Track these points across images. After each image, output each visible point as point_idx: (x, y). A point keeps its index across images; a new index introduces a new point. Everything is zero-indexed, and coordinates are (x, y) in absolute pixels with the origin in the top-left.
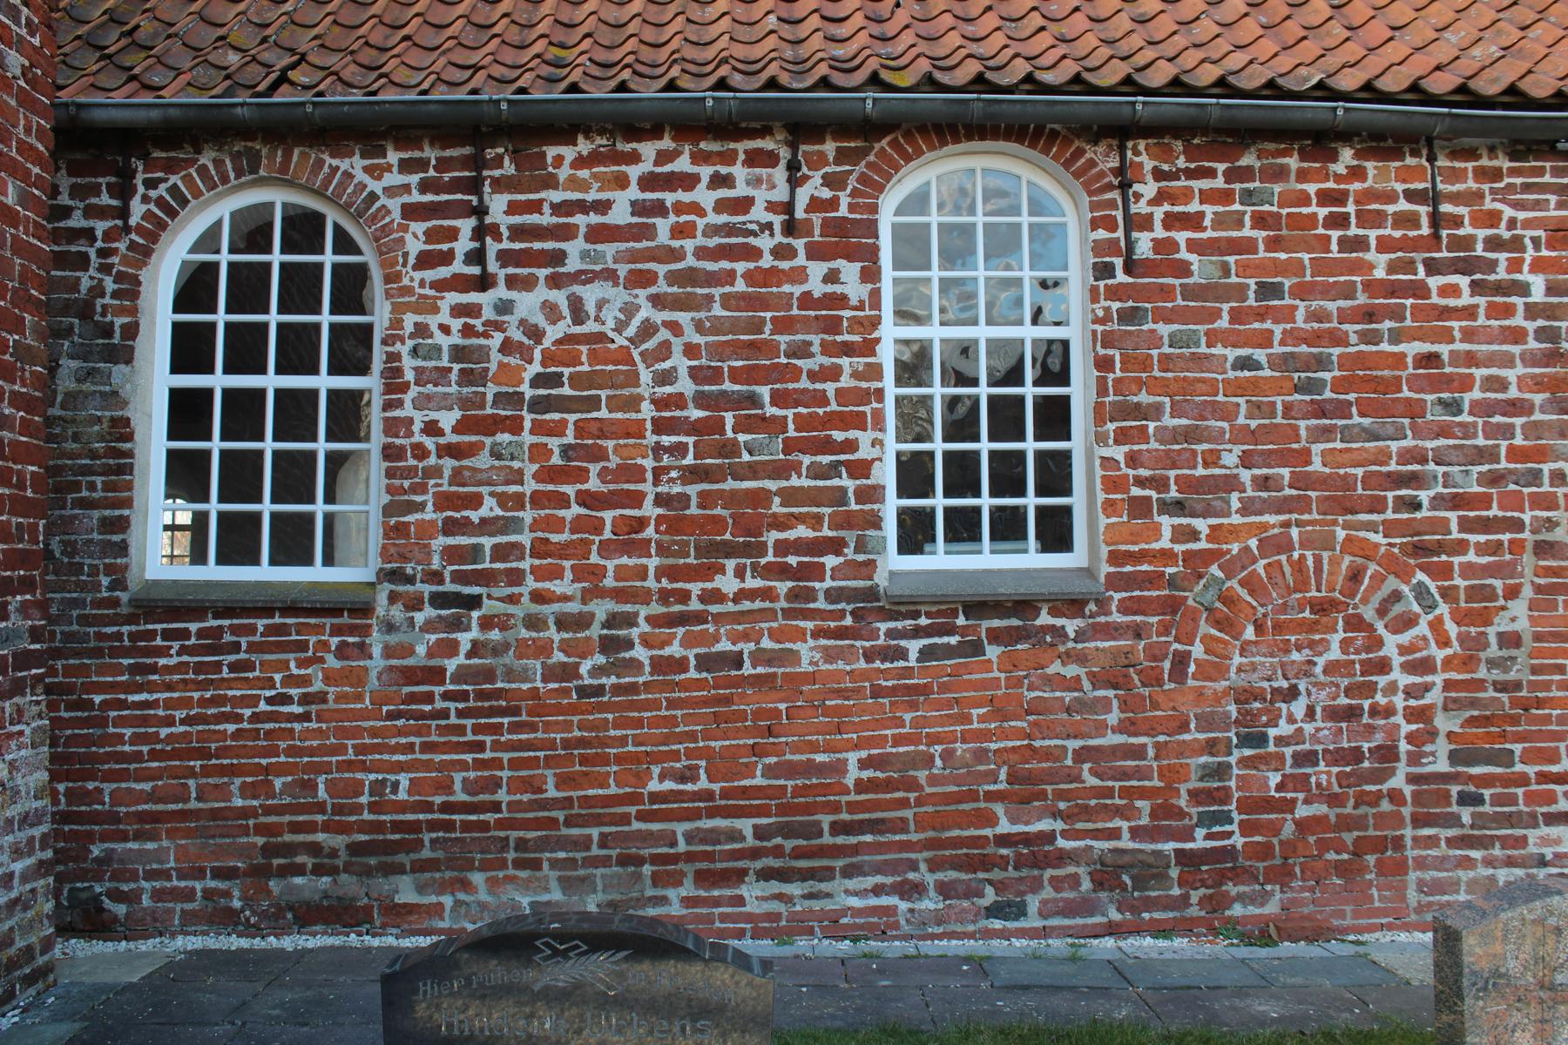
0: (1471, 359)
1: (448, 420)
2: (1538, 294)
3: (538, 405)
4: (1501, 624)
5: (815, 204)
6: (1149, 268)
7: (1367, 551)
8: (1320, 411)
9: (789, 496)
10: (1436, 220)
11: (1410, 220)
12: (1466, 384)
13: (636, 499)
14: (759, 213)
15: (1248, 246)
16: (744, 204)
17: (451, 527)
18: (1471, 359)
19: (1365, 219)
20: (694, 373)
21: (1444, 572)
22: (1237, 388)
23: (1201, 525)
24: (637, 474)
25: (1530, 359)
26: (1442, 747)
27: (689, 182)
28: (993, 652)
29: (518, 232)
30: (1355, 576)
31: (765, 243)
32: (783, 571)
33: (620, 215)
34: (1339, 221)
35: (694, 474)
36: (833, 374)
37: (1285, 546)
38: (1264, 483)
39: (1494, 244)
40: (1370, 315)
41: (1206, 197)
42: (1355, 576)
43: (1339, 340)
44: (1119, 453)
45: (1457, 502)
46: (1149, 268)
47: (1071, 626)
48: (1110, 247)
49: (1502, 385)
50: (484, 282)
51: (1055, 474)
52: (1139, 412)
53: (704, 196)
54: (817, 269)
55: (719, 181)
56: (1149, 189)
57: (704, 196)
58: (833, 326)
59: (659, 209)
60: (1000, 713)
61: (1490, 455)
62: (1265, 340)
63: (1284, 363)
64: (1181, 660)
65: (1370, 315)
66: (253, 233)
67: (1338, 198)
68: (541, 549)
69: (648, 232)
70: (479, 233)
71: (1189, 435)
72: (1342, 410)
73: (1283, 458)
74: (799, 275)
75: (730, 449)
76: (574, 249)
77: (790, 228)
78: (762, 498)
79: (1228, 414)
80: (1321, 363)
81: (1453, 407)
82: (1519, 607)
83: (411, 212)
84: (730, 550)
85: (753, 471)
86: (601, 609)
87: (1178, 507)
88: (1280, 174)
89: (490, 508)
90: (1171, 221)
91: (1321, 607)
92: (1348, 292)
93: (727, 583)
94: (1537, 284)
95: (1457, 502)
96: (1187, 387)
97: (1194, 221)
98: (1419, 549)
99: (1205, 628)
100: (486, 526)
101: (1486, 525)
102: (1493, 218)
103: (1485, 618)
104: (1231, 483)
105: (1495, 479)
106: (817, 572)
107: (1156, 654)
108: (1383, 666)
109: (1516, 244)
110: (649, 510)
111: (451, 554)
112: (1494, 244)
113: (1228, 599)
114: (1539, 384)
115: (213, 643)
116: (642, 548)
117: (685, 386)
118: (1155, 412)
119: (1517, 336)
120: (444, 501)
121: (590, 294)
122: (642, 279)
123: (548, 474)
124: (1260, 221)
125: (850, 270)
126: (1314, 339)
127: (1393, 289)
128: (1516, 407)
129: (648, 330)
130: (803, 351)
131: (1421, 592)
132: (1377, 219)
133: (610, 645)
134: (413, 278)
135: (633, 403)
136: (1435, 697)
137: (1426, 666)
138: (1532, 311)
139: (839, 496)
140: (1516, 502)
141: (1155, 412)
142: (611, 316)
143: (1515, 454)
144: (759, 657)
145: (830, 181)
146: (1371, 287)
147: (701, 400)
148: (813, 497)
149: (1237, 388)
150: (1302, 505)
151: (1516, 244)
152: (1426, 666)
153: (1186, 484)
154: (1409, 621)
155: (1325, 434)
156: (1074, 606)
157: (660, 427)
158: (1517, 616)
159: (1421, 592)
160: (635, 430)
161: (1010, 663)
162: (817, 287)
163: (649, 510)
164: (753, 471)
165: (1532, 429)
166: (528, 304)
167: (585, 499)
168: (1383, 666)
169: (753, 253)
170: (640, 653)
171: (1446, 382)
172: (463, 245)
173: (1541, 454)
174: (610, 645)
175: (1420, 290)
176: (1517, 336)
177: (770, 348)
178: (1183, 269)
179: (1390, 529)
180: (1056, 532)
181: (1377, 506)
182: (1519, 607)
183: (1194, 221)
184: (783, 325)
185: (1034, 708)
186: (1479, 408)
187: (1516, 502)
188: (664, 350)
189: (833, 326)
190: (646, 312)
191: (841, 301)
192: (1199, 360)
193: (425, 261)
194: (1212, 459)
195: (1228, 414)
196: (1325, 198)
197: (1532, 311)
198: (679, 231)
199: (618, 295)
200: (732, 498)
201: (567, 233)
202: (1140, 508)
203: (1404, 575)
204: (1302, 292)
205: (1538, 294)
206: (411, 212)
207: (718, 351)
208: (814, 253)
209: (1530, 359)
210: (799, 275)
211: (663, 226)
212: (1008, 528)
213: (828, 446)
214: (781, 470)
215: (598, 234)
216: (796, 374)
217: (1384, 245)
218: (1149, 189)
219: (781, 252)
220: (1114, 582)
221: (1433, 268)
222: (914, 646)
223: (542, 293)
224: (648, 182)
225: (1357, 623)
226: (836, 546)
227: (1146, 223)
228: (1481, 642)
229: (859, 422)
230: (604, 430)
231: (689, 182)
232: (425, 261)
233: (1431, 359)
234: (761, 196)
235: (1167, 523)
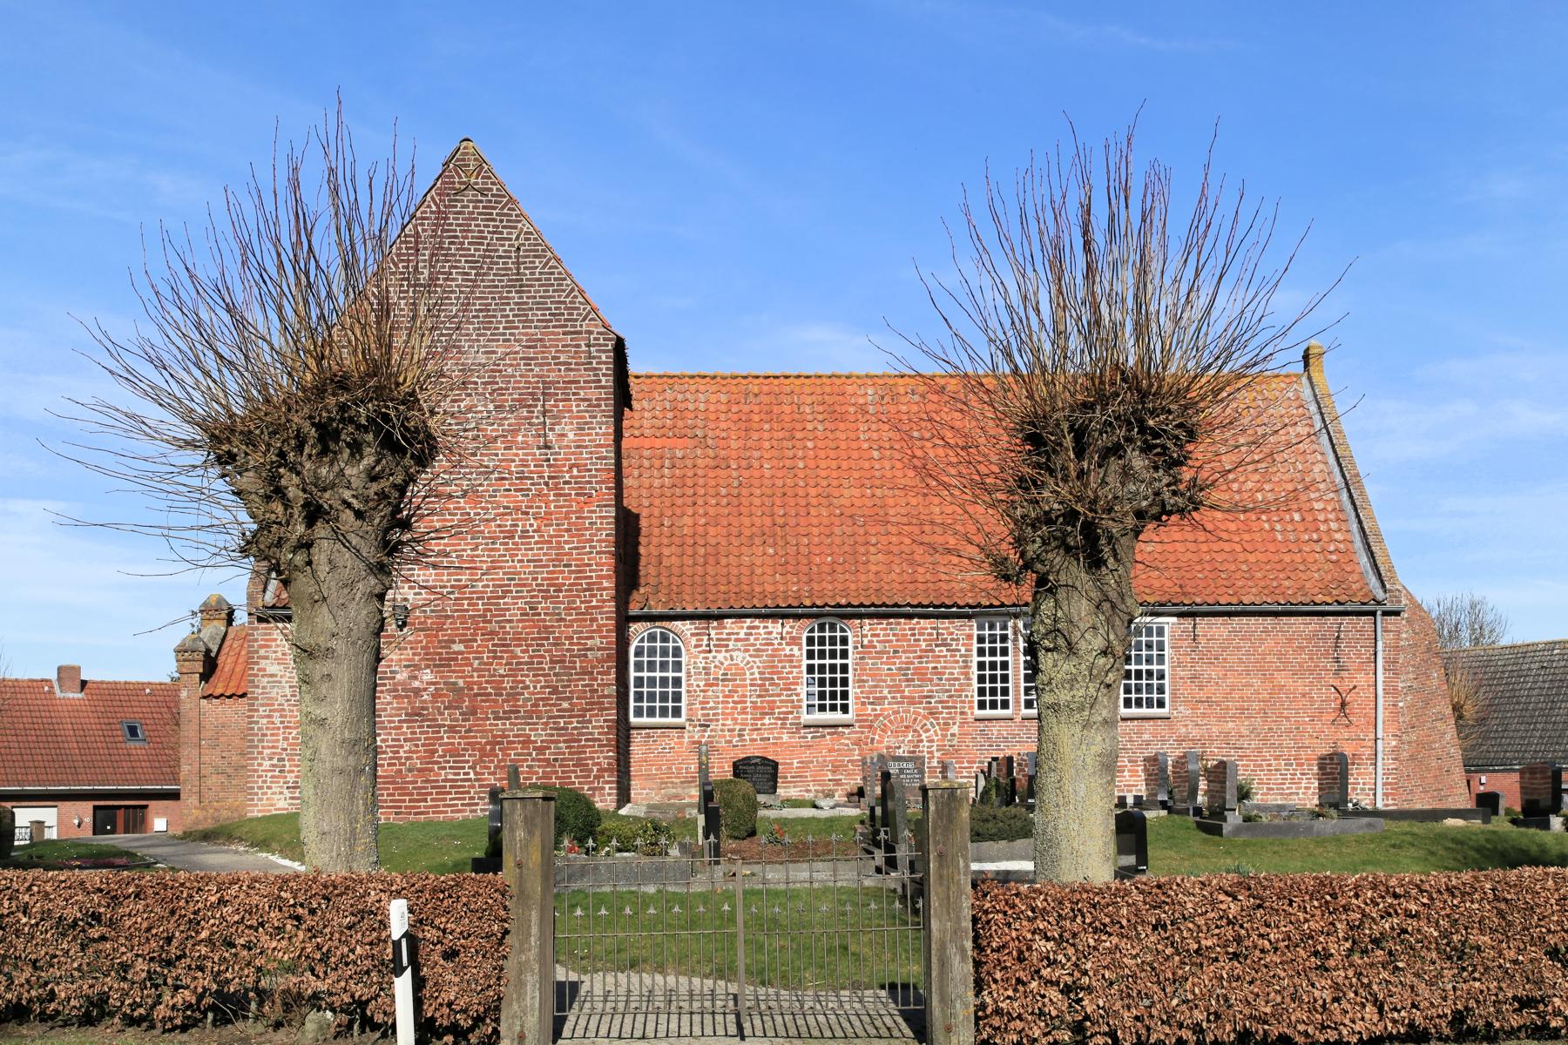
0: (945, 668)
1: (702, 683)
2: (963, 652)
3: (723, 680)
4: (951, 731)
5: (788, 633)
6: (867, 647)
7: (919, 714)
8: (908, 680)
9: (781, 701)
10: (938, 634)
11: (931, 634)
12: (944, 674)
13: (745, 702)
14: (774, 635)
15: (891, 641)
16: (770, 633)
17: (703, 709)
18: (945, 668)
19: (920, 634)
20: (760, 673)
21: (937, 719)
22: (887, 675)
23: (878, 707)
24: (746, 696)
25: (960, 668)
26: (935, 760)
27: (758, 627)
28: (828, 737)
29: (718, 640)
30: (915, 719)
31: (776, 642)
32: (780, 719)
33: (742, 636)
34: (914, 635)
35: (759, 696)
36: (791, 673)
37: (898, 712)
38: (893, 698)
39: (952, 639)
40: (920, 657)
41: (881, 629)
42: (915, 719)
43: (913, 663)
44: (858, 691)
45: (941, 702)
46: (867, 647)
47: (847, 731)
48: (857, 642)
49: (953, 674)
50: (710, 651)
51: (845, 695)
52: (863, 681)
53: (762, 631)
54: (788, 648)
55: (765, 627)
56: (867, 627)
57: (762, 631)
58: (792, 661)
59: (751, 634)
60: (830, 751)
61: (949, 691)
62: (895, 664)
63: (900, 669)
64: (873, 739)
65: (920, 657)
66: (652, 638)
67: (913, 629)
68: (723, 714)
69: (748, 640)
70: (709, 639)
71: (876, 686)
72: (913, 680)
73: (898, 692)
74: (784, 650)
75: (767, 690)
76: (731, 643)
77: (782, 638)
78: (775, 702)
79: (885, 681)
80: (908, 669)
81: (941, 679)
82: (956, 727)
83: (692, 635)
84: (767, 714)
85: (772, 695)
86: (738, 727)
87: (872, 703)
88: (899, 624)
89: (711, 704)
90: (873, 635)
91: (907, 727)
92: (915, 652)
93: (766, 721)
94: (963, 649)
95: (941, 702)
96: (875, 675)
97: (878, 635)
98: (931, 713)
99: (878, 732)
100: (711, 708)
101: (948, 708)
102: (952, 633)
103: (947, 730)
104: (886, 698)
105: (951, 696)
106: (787, 719)
107: (867, 738)
108: (922, 741)
109: (958, 640)
110: (749, 704)
111: (704, 715)
112: (952, 639)
113: (885, 725)
114: (962, 674)
115: (648, 736)
116: (747, 713)
117: (757, 676)
118: (867, 681)
119: (957, 662)
120: (701, 703)
121: (735, 654)
122: (748, 651)
123: (725, 696)
124: (894, 635)
125: (796, 648)
126: (907, 663)
127: (926, 651)
128: (958, 679)
129: (748, 663)
130: (784, 667)
131: (932, 724)
132: (923, 634)
133: (740, 735)
134: (693, 650)
135: (745, 680)
136: (934, 748)
137: (932, 741)
138: (961, 656)
139: (793, 701)
140: (956, 702)
141: (867, 681)
142: (740, 659)
143: (956, 690)
144: (774, 738)
145: (792, 627)
146: (921, 651)
147: (761, 679)
148: (786, 701)
149: (887, 675)
150: (903, 703)
151: (958, 640)
152: (932, 741)
153: (874, 698)
154: (928, 731)
155: (908, 686)
156: (848, 726)
157: (751, 685)
158: (955, 729)
159: (932, 724)
160: (745, 686)
161: (832, 740)
162: (788, 653)
163: (749, 704)
164: (772, 695)
165: (961, 685)
166: (720, 657)
167: (734, 702)
168: (922, 741)
169: (772, 644)
170: (747, 737)
171: (940, 673)
172: (705, 642)
173: (962, 691)
174: (740, 735)
175: (933, 651)
176: (957, 662)
177: (777, 667)
178: (875, 647)
179: (924, 708)
180: (845, 709)
181: (921, 703)
182: (956, 727)
183: (878, 635)
184: (780, 661)
185: (838, 750)
186: (947, 680)
187: (956, 702)
188: (752, 667)
189: (792, 661)
190: (748, 658)
191: (793, 655)
192: (878, 669)
193: (696, 646)
194: (881, 692)
195: (885, 681)
196: (910, 629)
197: (961, 656)
198: (756, 639)
199: (741, 654)
200: (768, 702)
201: (729, 640)
202: (863, 704)
203: (928, 719)
204: (904, 652)
205: (963, 652)
206: (692, 635)
207: (764, 667)
208: (787, 644)
209: (960, 668)
210: (784, 650)
211: (752, 638)
212: (833, 708)
213: (790, 689)
214: (779, 695)
215: (737, 640)
216: (782, 672)
217: (925, 640)
218: (867, 627)
219: (780, 644)
220: (857, 721)
221: (937, 646)
222: (810, 736)
223: (724, 654)
224: (749, 628)
225: (915, 731)
226: (792, 713)
227: (866, 636)
228: (946, 736)
229: (797, 684)
230: (738, 686)
231: (758, 627)
232: (696, 646)
233: (935, 668)
234: (775, 631)
235: (870, 707)
